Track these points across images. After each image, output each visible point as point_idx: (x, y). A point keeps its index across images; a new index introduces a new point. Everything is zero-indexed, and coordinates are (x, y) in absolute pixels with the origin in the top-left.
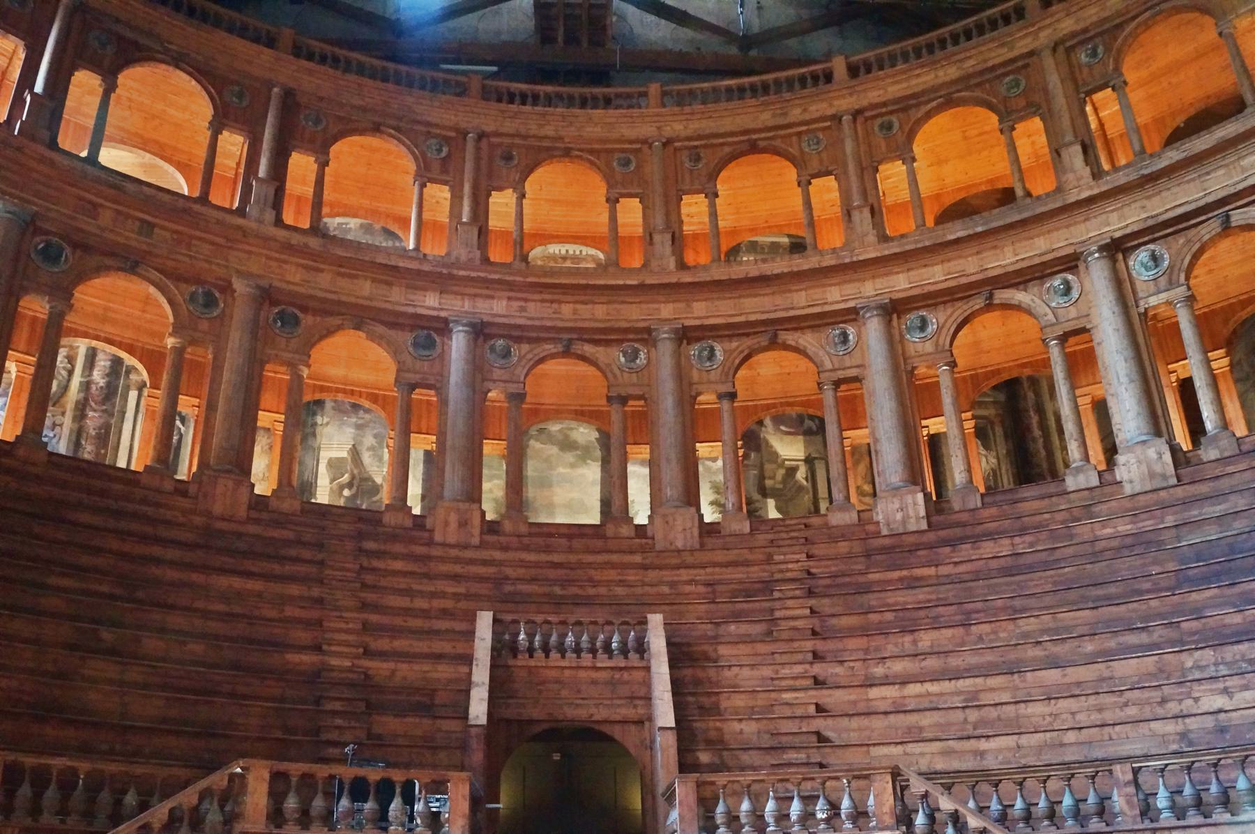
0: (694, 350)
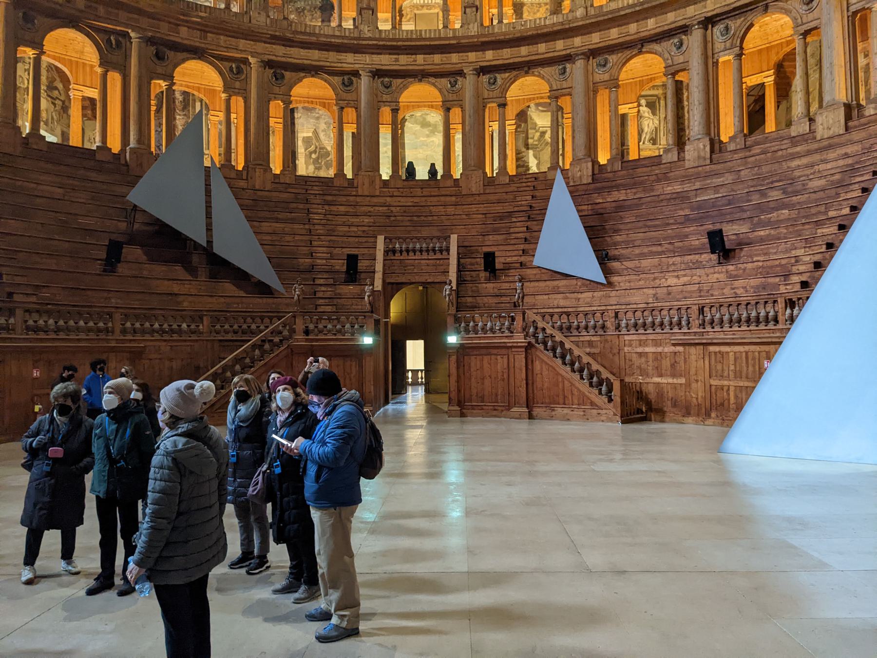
0: (485, 78)
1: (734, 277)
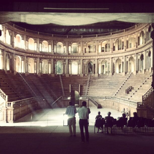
0: (84, 60)
1: (111, 93)
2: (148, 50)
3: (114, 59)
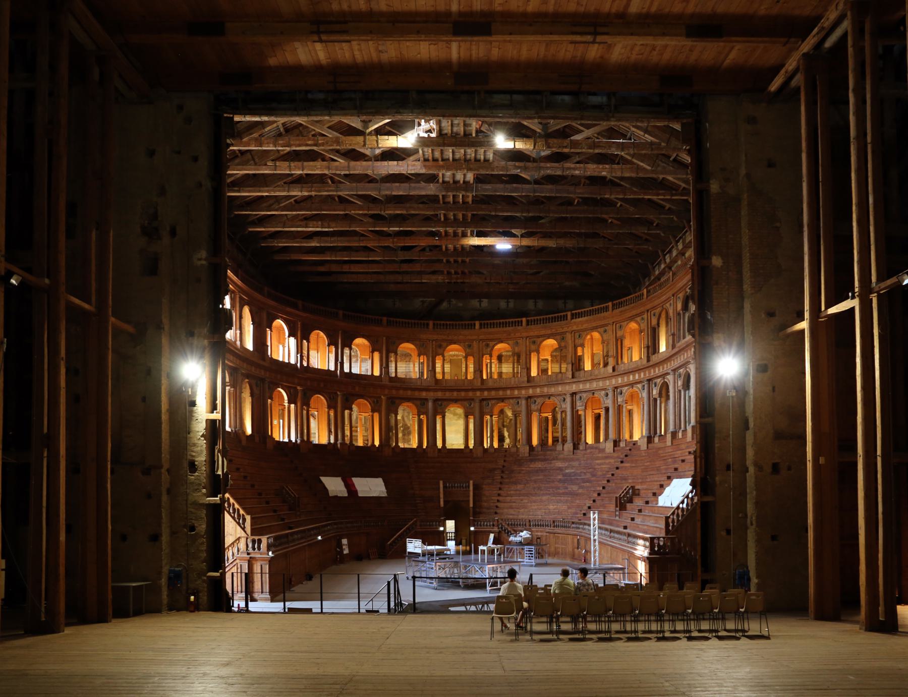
1: (569, 508)
2: (681, 370)
3: (578, 397)
